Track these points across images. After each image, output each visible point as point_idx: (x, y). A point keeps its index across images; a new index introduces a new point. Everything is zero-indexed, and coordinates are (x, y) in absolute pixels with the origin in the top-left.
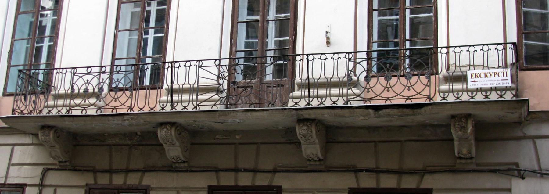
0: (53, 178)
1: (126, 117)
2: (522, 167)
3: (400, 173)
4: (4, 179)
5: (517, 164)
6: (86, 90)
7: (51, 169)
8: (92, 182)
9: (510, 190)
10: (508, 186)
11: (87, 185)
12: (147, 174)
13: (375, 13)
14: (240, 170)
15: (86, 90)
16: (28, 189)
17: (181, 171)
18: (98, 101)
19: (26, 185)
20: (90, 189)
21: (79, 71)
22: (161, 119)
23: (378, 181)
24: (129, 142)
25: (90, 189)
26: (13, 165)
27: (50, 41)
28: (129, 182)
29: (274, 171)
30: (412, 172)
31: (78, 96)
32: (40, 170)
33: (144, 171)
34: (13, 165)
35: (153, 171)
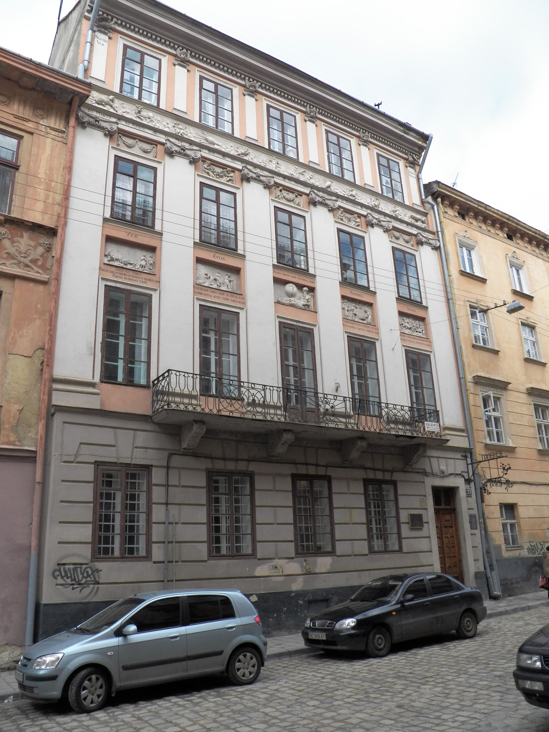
0: (176, 461)
1: (268, 423)
2: (427, 471)
3: (384, 471)
4: (130, 459)
5: (425, 469)
6: (254, 400)
7: (174, 454)
8: (210, 466)
9: (424, 482)
10: (422, 480)
11: (206, 469)
12: (251, 463)
13: (356, 378)
14: (319, 466)
15: (254, 400)
16: (154, 469)
17: (275, 462)
18: (229, 406)
19: (152, 466)
20: (209, 472)
21: (257, 386)
22: (284, 427)
23: (375, 475)
24: (234, 438)
25: (209, 472)
26: (137, 447)
27: (216, 356)
28: (239, 468)
29: (326, 466)
30: (387, 471)
31: (259, 405)
32: (165, 454)
33: (249, 460)
34: (137, 447)
35: (278, 463)
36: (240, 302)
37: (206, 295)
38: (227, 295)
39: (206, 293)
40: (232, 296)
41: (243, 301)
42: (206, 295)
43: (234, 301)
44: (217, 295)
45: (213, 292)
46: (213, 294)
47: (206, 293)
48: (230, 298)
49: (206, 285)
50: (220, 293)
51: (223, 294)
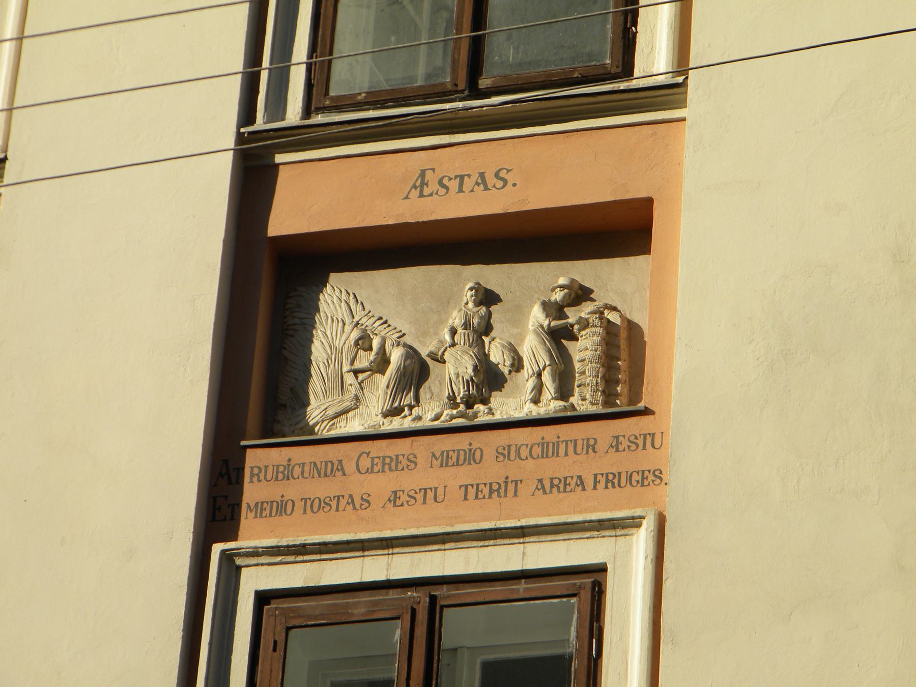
36: (612, 480)
37: (324, 504)
38: (504, 454)
39: (322, 489)
40: (548, 450)
41: (645, 460)
42: (324, 504)
43: (561, 485)
44: (409, 481)
45: (392, 464)
46: (380, 485)
47: (322, 489)
48: (530, 469)
49: (354, 425)
50: (445, 460)
51: (471, 457)
